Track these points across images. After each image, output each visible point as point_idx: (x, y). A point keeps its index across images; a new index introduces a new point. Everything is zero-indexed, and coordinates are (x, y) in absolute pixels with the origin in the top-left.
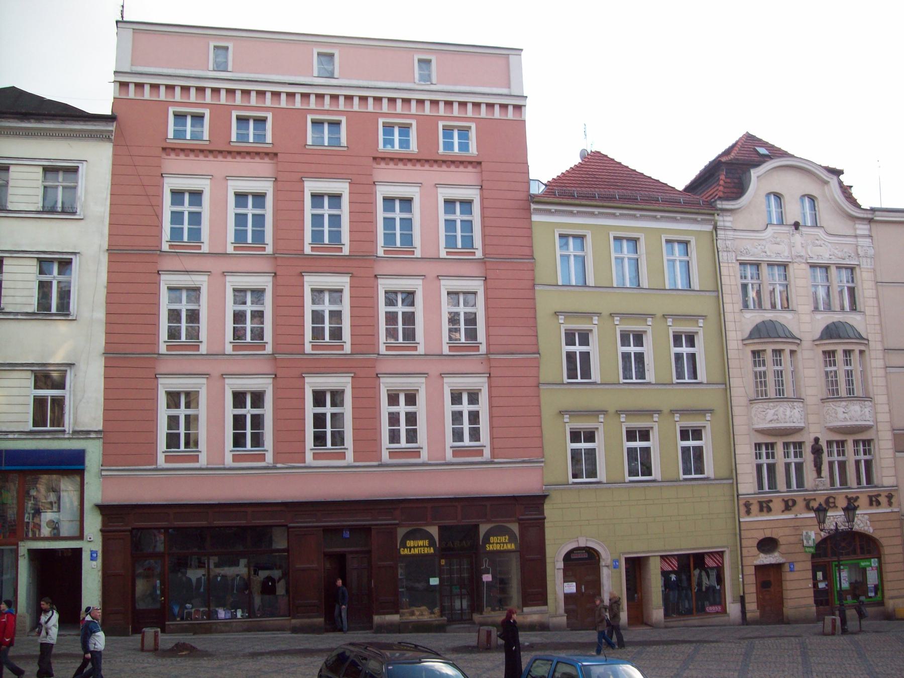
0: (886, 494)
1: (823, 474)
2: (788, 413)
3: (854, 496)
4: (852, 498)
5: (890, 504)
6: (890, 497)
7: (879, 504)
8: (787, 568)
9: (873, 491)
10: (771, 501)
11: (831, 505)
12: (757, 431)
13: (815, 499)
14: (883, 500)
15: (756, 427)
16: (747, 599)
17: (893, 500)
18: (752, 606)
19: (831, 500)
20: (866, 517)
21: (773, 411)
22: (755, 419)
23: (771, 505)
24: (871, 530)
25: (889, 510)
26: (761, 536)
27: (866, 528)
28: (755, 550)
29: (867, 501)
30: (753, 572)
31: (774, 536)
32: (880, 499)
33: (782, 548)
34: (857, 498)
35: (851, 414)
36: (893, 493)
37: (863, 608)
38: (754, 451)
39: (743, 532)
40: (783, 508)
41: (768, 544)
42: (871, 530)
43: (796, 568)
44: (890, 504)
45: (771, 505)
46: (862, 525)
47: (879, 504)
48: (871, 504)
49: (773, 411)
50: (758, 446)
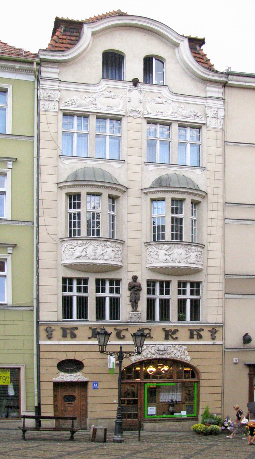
1: (139, 308)
3: (173, 329)
8: (90, 386)
10: (77, 328)
13: (127, 330)
15: (64, 262)
20: (184, 347)
21: (82, 248)
22: (64, 255)
23: (76, 332)
26: (63, 357)
27: (183, 357)
28: (56, 370)
30: (51, 386)
31: (77, 358)
33: (85, 369)
34: (177, 331)
37: (142, 423)
38: (61, 285)
39: (41, 353)
40: (90, 336)
41: (70, 365)
42: (189, 358)
45: (76, 332)
46: (178, 354)
48: (191, 337)
49: (82, 248)
50: (65, 280)
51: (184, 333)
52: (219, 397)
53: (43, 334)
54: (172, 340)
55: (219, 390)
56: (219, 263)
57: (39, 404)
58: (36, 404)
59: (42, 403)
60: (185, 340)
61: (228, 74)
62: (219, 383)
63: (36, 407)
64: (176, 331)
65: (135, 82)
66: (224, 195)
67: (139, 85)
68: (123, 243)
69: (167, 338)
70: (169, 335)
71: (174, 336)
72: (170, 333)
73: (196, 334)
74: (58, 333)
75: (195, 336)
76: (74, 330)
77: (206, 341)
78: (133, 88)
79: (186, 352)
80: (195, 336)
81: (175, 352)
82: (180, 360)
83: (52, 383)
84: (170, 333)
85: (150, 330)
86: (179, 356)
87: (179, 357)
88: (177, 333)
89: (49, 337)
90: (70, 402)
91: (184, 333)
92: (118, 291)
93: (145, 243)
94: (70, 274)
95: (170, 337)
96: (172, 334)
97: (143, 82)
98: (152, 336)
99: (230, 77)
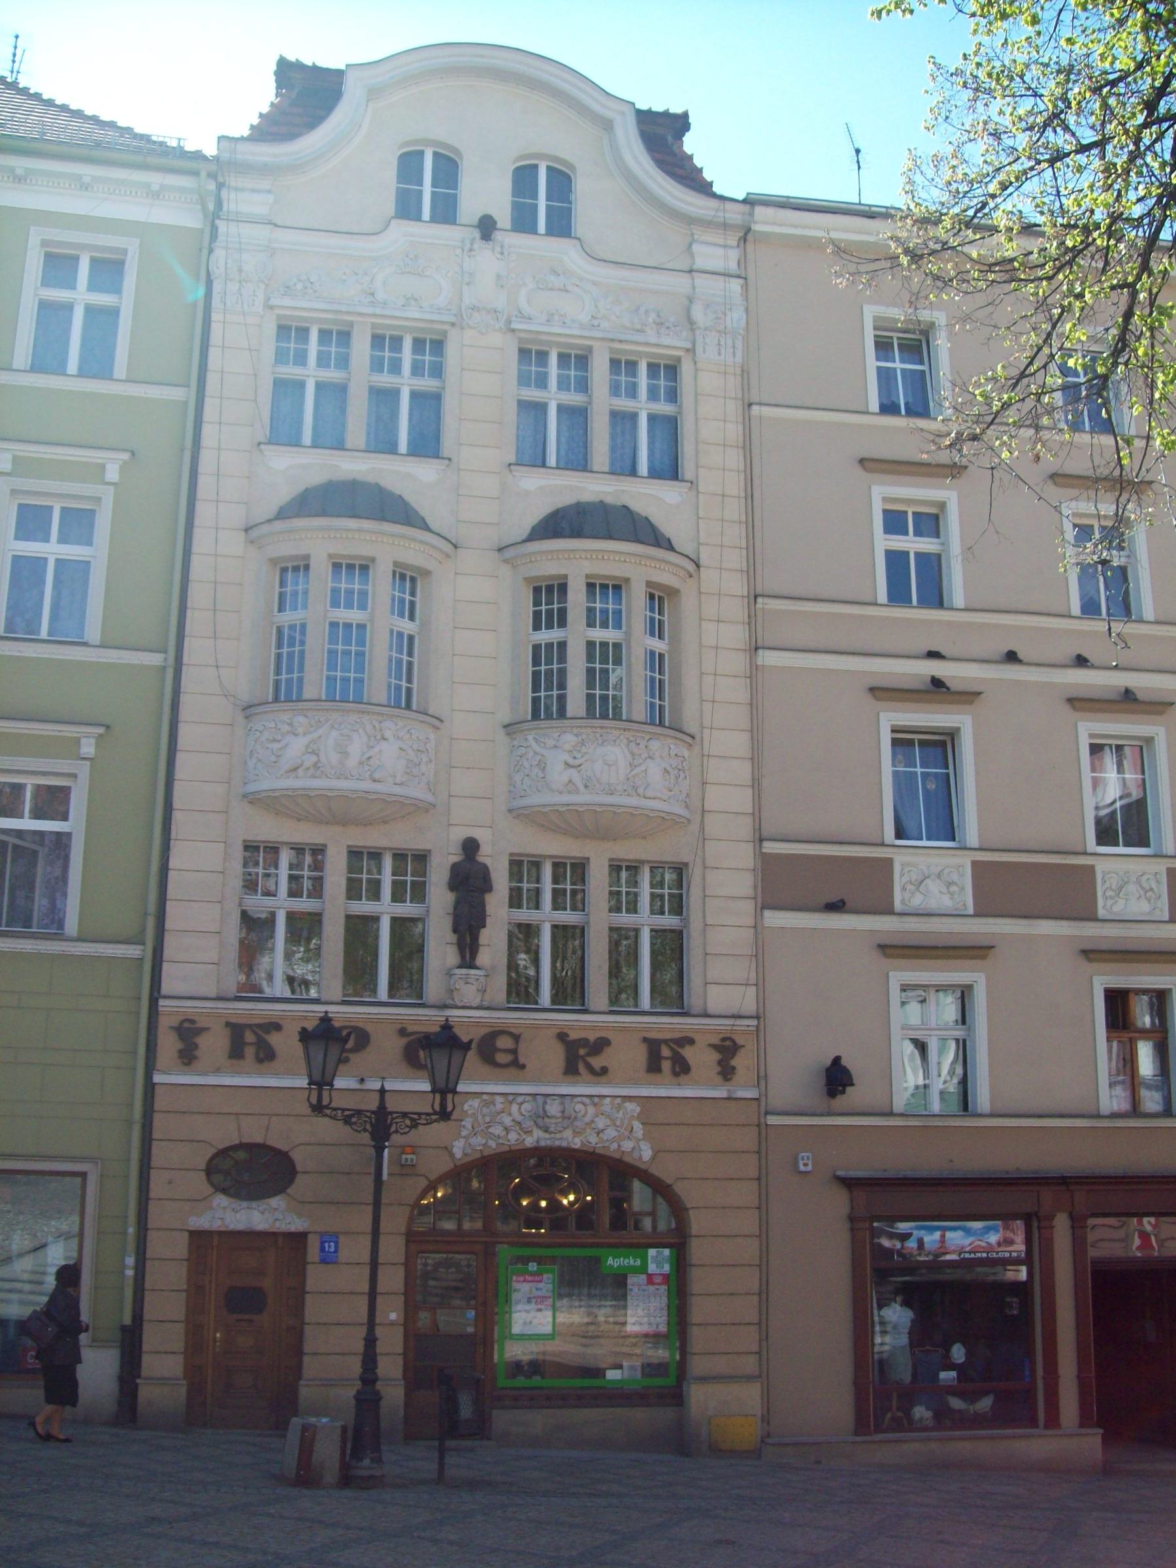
0: (715, 1040)
2: (356, 748)
3: (592, 1037)
4: (584, 1042)
5: (727, 1072)
6: (727, 1049)
7: (682, 1068)
9: (668, 1025)
11: (502, 1058)
12: (254, 800)
14: (701, 1057)
16: (151, 1338)
18: (164, 1362)
19: (504, 1042)
20: (633, 1108)
24: (647, 1153)
25: (720, 1093)
29: (640, 1055)
32: (687, 1052)
35: (598, 768)
36: (740, 1040)
38: (236, 868)
39: (157, 1119)
43: (343, 1255)
44: (727, 1072)
47: (682, 1068)
48: (654, 1066)
50: (250, 848)
53: (168, 1044)
54: (591, 1077)
56: (742, 800)
57: (138, 1317)
58: (127, 1320)
59: (147, 1316)
60: (637, 1083)
61: (751, 202)
63: (124, 1329)
64: (600, 1045)
65: (486, 227)
66: (751, 571)
67: (498, 236)
68: (437, 723)
69: (571, 1069)
70: (581, 1056)
71: (596, 1062)
72: (582, 1052)
73: (666, 1057)
74: (214, 1044)
75: (666, 1065)
76: (268, 1032)
77: (701, 1087)
78: (479, 244)
79: (637, 1125)
80: (666, 1065)
81: (601, 1125)
82: (617, 1156)
83: (187, 1234)
84: (582, 1052)
85: (516, 1038)
86: (613, 1140)
87: (614, 1146)
88: (608, 1051)
89: (188, 1056)
90: (247, 1317)
92: (419, 892)
93: (505, 727)
94: (268, 829)
95: (581, 1068)
96: (589, 1054)
97: (509, 227)
98: (522, 1060)
99: (758, 210)
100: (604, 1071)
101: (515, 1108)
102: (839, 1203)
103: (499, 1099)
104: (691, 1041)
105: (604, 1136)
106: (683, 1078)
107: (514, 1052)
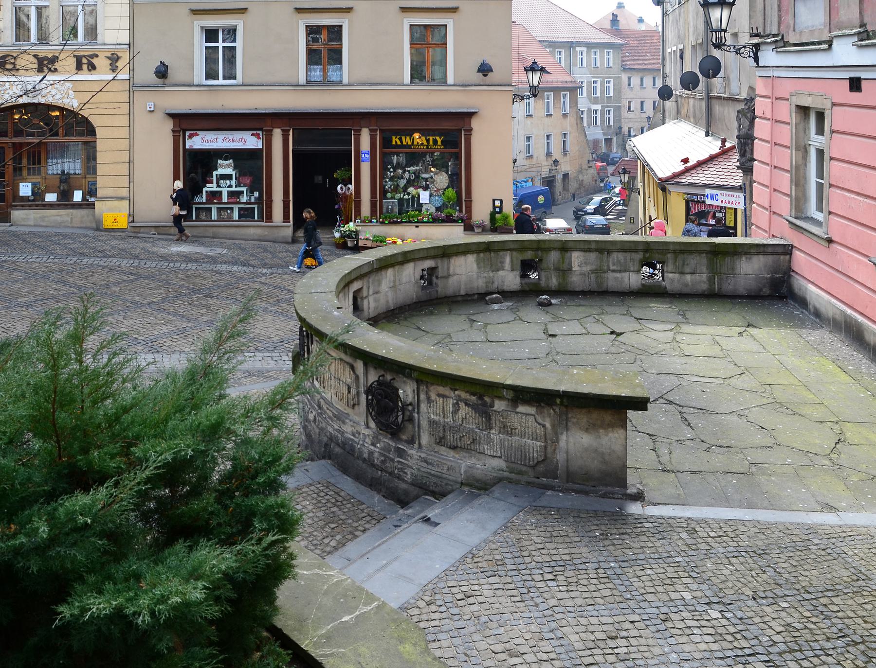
4: (46, 58)
5: (114, 69)
6: (114, 59)
7: (92, 67)
14: (101, 62)
17: (120, 64)
20: (68, 84)
27: (66, 101)
32: (95, 61)
36: (119, 54)
46: (58, 96)
47: (92, 67)
48: (79, 67)
51: (67, 63)
52: (125, 169)
55: (125, 157)
62: (125, 144)
64: (54, 60)
72: (45, 62)
75: (85, 67)
77: (103, 74)
79: (71, 92)
80: (85, 67)
81: (53, 93)
84: (45, 62)
91: (67, 63)
100: (56, 70)
101: (14, 88)
102: (169, 125)
103: (7, 84)
104: (97, 56)
105: (57, 97)
106: (93, 72)
107: (14, 64)
